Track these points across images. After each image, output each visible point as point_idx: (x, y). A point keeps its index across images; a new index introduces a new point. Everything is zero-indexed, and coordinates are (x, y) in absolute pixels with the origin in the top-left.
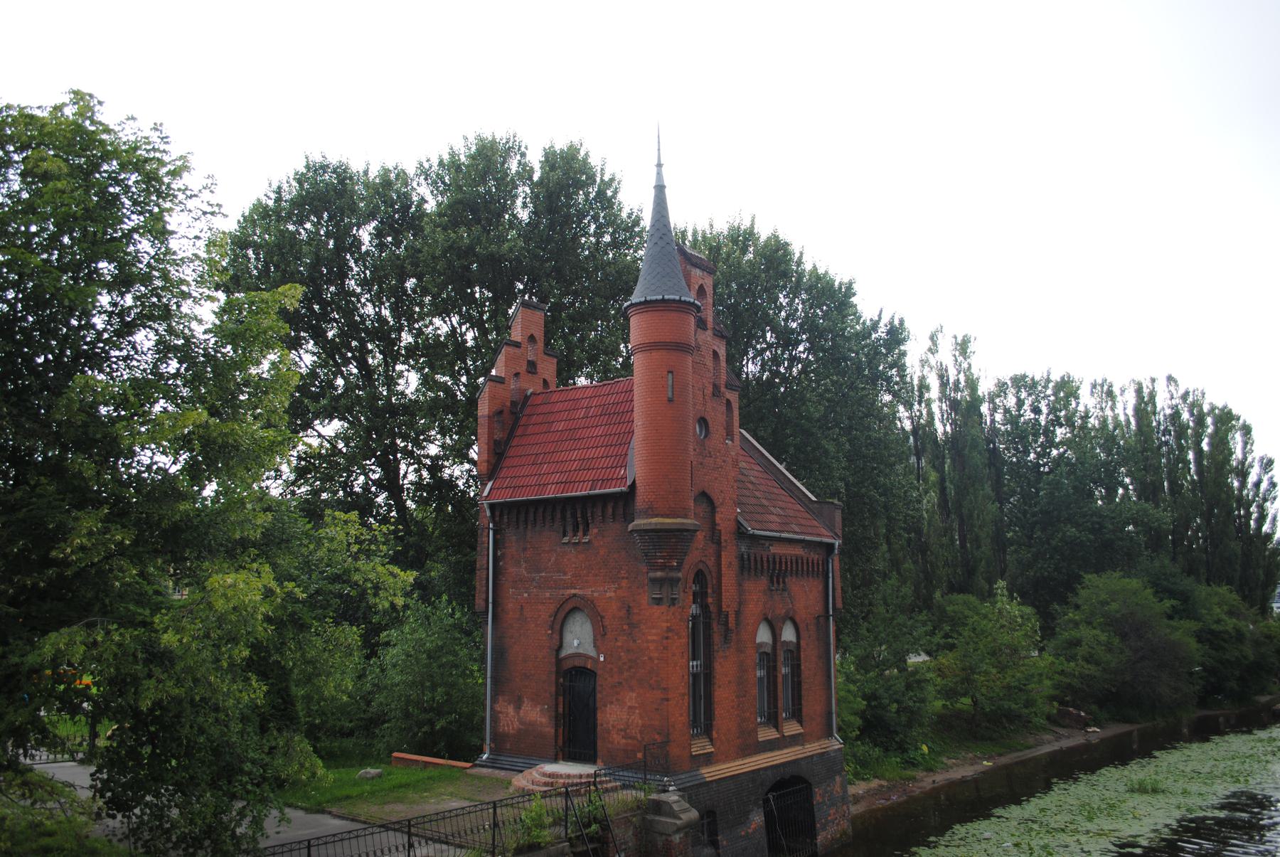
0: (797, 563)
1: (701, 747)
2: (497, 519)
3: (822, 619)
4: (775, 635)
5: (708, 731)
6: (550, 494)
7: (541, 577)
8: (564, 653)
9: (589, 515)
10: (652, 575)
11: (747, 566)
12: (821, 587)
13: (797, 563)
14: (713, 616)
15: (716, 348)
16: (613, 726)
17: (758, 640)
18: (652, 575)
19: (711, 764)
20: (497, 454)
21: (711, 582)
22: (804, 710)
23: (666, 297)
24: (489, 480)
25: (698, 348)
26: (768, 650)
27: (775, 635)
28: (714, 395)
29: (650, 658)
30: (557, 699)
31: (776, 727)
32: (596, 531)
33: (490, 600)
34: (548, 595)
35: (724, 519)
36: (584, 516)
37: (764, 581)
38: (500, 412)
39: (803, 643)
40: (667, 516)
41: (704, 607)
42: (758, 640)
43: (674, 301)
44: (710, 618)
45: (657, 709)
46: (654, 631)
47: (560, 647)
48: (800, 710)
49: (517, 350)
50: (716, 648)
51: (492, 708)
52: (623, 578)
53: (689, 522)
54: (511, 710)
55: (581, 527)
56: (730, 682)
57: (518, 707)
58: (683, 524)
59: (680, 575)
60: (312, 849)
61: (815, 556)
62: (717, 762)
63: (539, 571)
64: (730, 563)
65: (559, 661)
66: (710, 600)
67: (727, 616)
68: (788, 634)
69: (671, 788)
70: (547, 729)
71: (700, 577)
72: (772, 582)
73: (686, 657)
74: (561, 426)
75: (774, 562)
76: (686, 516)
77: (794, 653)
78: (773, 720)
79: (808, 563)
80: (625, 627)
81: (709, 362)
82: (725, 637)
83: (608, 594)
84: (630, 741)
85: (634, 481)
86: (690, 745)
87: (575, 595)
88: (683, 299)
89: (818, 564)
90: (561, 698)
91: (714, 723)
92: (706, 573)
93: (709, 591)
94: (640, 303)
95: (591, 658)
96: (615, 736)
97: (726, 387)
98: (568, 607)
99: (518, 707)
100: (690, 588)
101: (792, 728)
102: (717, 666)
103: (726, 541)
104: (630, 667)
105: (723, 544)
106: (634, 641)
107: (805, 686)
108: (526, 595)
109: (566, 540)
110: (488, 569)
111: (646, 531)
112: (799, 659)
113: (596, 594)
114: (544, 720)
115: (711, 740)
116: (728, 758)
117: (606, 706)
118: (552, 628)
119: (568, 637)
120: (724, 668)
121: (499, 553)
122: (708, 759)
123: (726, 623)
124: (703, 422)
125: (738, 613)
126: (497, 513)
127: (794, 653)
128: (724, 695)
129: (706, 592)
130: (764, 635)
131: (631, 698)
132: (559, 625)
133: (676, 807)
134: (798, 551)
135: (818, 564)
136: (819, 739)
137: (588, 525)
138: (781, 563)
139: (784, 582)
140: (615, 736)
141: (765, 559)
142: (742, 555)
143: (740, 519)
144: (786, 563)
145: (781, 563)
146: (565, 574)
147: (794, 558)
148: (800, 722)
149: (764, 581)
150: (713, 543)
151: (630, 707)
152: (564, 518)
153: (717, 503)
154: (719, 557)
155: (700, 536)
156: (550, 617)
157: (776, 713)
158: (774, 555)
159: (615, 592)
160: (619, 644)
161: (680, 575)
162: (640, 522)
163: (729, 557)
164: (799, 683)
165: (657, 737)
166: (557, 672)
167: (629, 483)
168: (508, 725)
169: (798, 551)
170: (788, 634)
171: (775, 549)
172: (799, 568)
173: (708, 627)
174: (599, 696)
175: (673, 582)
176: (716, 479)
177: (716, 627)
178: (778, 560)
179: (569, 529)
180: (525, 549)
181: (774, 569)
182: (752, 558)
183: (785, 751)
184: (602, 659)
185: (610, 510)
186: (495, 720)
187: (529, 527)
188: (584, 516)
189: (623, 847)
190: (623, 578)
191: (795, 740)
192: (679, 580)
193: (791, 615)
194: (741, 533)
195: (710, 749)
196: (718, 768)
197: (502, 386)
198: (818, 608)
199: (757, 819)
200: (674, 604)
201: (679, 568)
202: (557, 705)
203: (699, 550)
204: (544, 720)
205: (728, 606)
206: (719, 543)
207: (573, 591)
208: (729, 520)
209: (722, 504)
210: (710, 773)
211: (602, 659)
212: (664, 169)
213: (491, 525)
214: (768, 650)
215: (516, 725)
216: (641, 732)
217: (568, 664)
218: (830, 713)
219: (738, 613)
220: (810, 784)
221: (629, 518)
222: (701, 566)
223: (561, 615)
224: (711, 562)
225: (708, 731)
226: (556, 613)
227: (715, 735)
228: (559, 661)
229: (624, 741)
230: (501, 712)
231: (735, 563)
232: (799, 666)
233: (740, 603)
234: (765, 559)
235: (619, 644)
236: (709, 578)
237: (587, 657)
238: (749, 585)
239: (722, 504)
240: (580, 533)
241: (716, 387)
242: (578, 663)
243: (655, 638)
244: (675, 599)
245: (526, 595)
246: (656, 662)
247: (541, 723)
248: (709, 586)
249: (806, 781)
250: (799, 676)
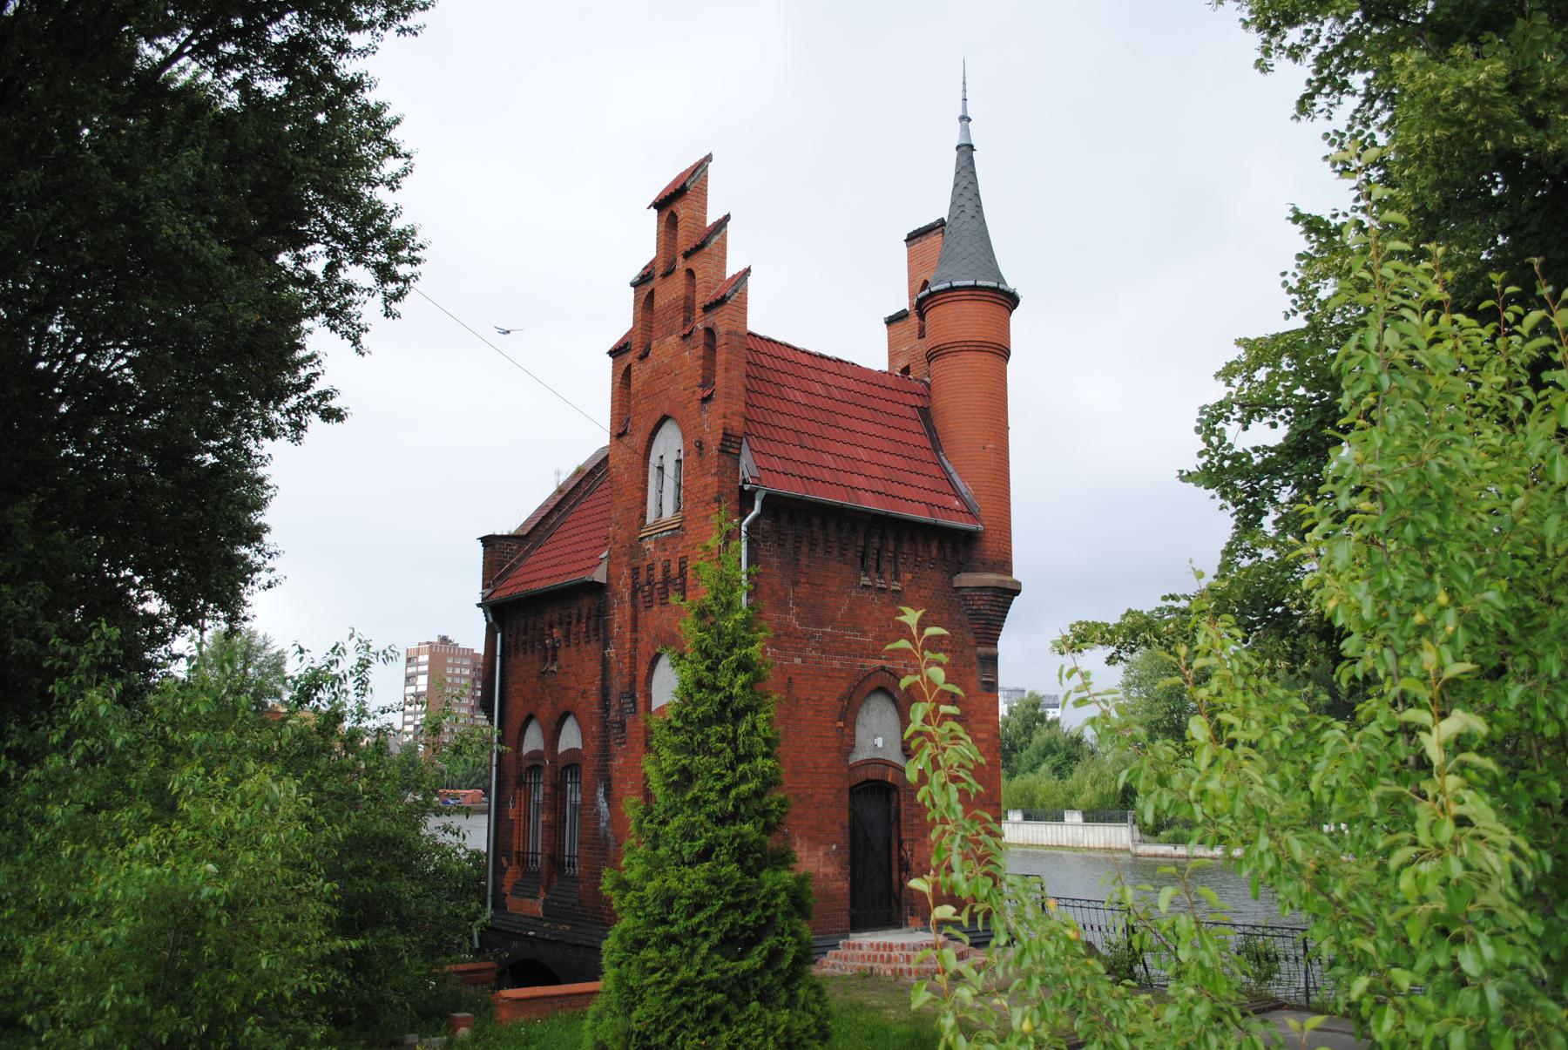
6: (870, 503)
7: (824, 633)
34: (836, 664)
46: (984, 726)
63: (821, 622)
70: (839, 884)
87: (883, 668)
95: (894, 766)
108: (798, 661)
114: (830, 870)
119: (861, 734)
132: (848, 715)
146: (864, 634)
156: (841, 699)
180: (796, 584)
187: (805, 549)
204: (830, 870)
237: (887, 764)
242: (873, 773)
245: (798, 661)
247: (826, 875)
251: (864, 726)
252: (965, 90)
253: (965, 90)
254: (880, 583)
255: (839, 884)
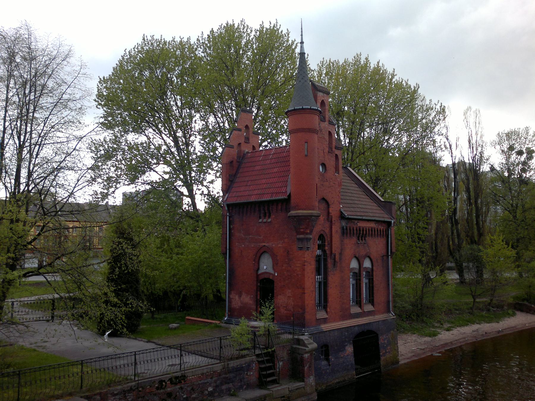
0: (372, 231)
1: (322, 314)
2: (231, 211)
3: (385, 258)
4: (360, 264)
5: (325, 308)
6: (253, 199)
8: (260, 272)
9: (271, 209)
10: (298, 236)
11: (345, 232)
12: (385, 242)
13: (372, 231)
14: (328, 255)
15: (330, 130)
16: (281, 305)
17: (351, 266)
18: (298, 236)
19: (327, 323)
20: (230, 181)
21: (327, 239)
22: (375, 300)
23: (304, 107)
24: (227, 193)
25: (321, 130)
26: (357, 271)
27: (360, 264)
28: (329, 152)
29: (297, 275)
30: (257, 293)
31: (360, 307)
32: (274, 216)
33: (228, 248)
34: (253, 246)
35: (334, 212)
36: (268, 209)
37: (354, 239)
38: (232, 162)
39: (374, 268)
40: (305, 210)
41: (324, 251)
42: (351, 266)
43: (308, 109)
44: (326, 256)
45: (300, 298)
46: (299, 262)
47: (258, 269)
48: (373, 300)
49: (240, 133)
50: (329, 270)
51: (229, 297)
52: (286, 238)
53: (315, 212)
54: (237, 297)
55: (267, 214)
56: (336, 286)
57: (240, 296)
58: (312, 213)
59: (311, 236)
60: (136, 356)
61: (381, 227)
62: (330, 322)
64: (337, 231)
65: (258, 276)
66: (326, 248)
67: (335, 256)
68: (367, 264)
69: (306, 334)
70: (253, 306)
71: (321, 237)
72: (359, 239)
73: (314, 274)
74: (258, 168)
75: (360, 230)
76: (313, 209)
77: (370, 274)
78: (359, 303)
79: (378, 231)
80: (287, 260)
81: (327, 137)
82: (334, 265)
83: (279, 245)
84: (288, 312)
85: (290, 193)
86: (316, 314)
87: (264, 246)
88: (312, 107)
89: (383, 231)
90: (259, 293)
91: (328, 304)
92: (325, 235)
93: (326, 244)
94: (292, 110)
95: (272, 274)
96: (282, 310)
97: (336, 149)
98: (262, 251)
99: (240, 296)
100: (316, 242)
101: (368, 308)
102: (330, 278)
103: (334, 221)
104: (289, 278)
105: (333, 222)
106: (290, 267)
107: (375, 289)
108: (243, 246)
109: (260, 220)
110: (227, 234)
111: (295, 216)
112: (372, 276)
113: (274, 245)
114: (251, 302)
115: (327, 312)
116: (335, 321)
117: (278, 296)
118: (254, 261)
119: (261, 266)
120: (334, 279)
121: (232, 227)
122: (325, 321)
123: (335, 259)
124: (323, 165)
125: (341, 254)
126: (231, 208)
127: (370, 274)
128: (333, 292)
129: (325, 245)
130: (354, 264)
131: (289, 292)
133: (306, 342)
134: (372, 225)
135: (383, 231)
136: (383, 313)
137: (270, 213)
138: (363, 230)
139: (365, 240)
140: (282, 310)
141: (355, 229)
142: (343, 227)
143: (342, 210)
144: (366, 231)
145: (363, 230)
147: (370, 229)
148: (373, 305)
149: (354, 239)
150: (328, 221)
151: (289, 297)
152: (260, 211)
153: (329, 202)
154: (331, 228)
155: (322, 218)
157: (360, 301)
158: (360, 227)
159: (282, 244)
160: (284, 268)
161: (311, 236)
162: (293, 213)
163: (336, 228)
164: (373, 287)
165: (300, 310)
166: (257, 281)
167: (288, 194)
168: (236, 304)
169: (372, 225)
170: (367, 264)
171: (361, 224)
172: (372, 233)
173: (325, 260)
174: (275, 291)
175: (308, 240)
176: (330, 192)
177: (329, 261)
178: (361, 229)
179: (262, 215)
181: (360, 233)
182: (348, 229)
183: (365, 318)
184: (276, 275)
185: (280, 207)
186: (230, 302)
188: (268, 209)
189: (282, 359)
190: (286, 238)
191: (370, 313)
192: (310, 239)
193: (368, 255)
194: (342, 217)
195: (326, 316)
196: (330, 325)
197: (233, 149)
198: (383, 252)
199: (350, 349)
200: (308, 250)
201: (310, 233)
202: (257, 296)
203: (320, 226)
204: (251, 302)
205: (335, 251)
206: (331, 222)
207: (264, 244)
208: (336, 211)
209: (333, 203)
210: (325, 327)
211: (276, 275)
212: (304, 45)
213: (228, 214)
214: (357, 271)
215: (239, 304)
216: (293, 308)
217: (261, 277)
218: (388, 302)
219: (341, 254)
220: (377, 335)
221: (288, 210)
222: (322, 232)
223: (258, 255)
224: (327, 231)
225: (325, 308)
226: (257, 254)
227: (328, 310)
228: (258, 276)
229: (286, 312)
230: (233, 299)
231: (340, 231)
232: (373, 279)
233: (342, 250)
234: (355, 229)
235: (284, 268)
236: (326, 238)
237: (270, 274)
238: (347, 241)
239: (333, 203)
240: (267, 217)
241: (330, 148)
242: (266, 276)
243: (299, 265)
244: (309, 247)
245: (243, 246)
246: (300, 276)
248: (326, 241)
249: (375, 333)
250: (373, 284)
251: (263, 263)
252: (302, 31)
253: (302, 31)
254: (265, 220)
255: (253, 306)
